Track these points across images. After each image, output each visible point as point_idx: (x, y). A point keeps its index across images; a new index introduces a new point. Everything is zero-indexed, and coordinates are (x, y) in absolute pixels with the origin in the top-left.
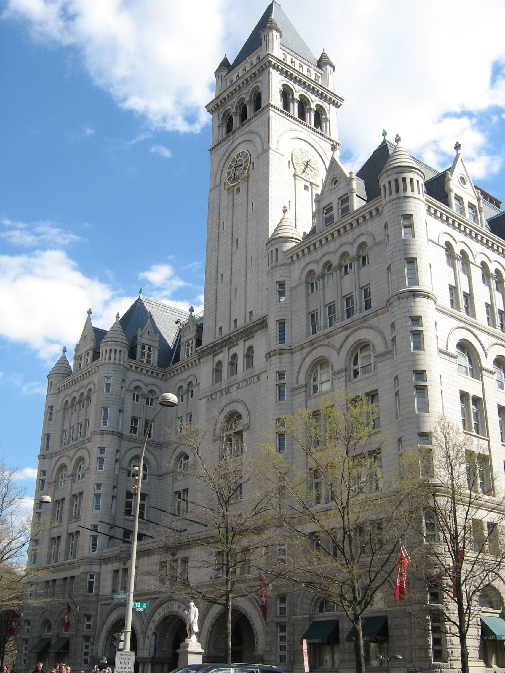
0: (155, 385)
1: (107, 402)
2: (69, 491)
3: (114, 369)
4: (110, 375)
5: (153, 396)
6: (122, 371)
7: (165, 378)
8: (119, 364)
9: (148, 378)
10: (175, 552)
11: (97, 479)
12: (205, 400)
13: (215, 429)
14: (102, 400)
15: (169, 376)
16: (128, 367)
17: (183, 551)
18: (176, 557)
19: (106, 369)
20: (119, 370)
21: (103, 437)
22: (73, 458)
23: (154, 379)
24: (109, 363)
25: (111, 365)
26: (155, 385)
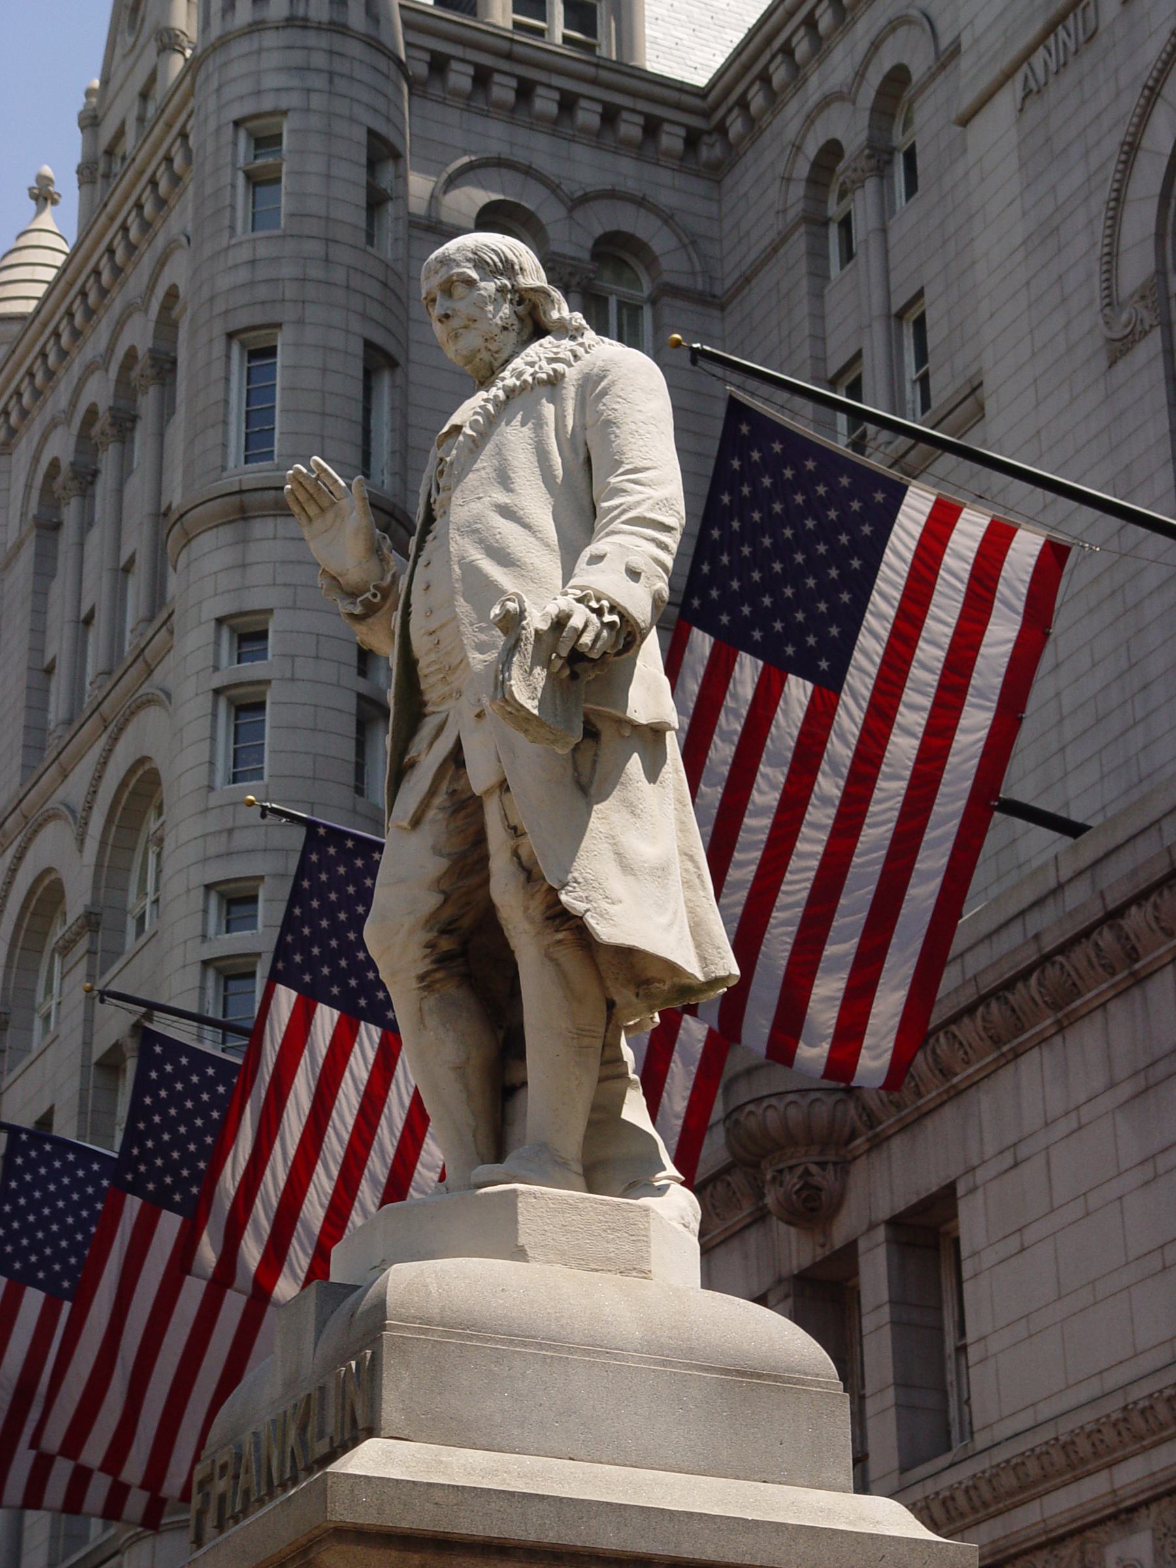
0: (641, 202)
1: (263, 292)
2: (77, 1038)
3: (297, 57)
4: (268, 104)
5: (636, 283)
6: (361, 73)
7: (710, 151)
8: (339, 28)
9: (582, 153)
10: (826, 1179)
11: (217, 845)
12: (1007, 101)
13: (1111, 258)
14: (224, 282)
15: (736, 127)
16: (420, 69)
17: (897, 1145)
18: (843, 1229)
19: (236, 69)
20: (341, 66)
21: (244, 541)
22: (89, 808)
23: (627, 165)
24: (256, 27)
25: (271, 39)
26: (641, 202)
